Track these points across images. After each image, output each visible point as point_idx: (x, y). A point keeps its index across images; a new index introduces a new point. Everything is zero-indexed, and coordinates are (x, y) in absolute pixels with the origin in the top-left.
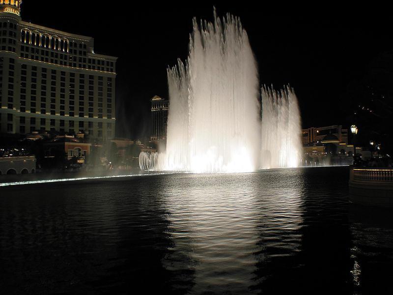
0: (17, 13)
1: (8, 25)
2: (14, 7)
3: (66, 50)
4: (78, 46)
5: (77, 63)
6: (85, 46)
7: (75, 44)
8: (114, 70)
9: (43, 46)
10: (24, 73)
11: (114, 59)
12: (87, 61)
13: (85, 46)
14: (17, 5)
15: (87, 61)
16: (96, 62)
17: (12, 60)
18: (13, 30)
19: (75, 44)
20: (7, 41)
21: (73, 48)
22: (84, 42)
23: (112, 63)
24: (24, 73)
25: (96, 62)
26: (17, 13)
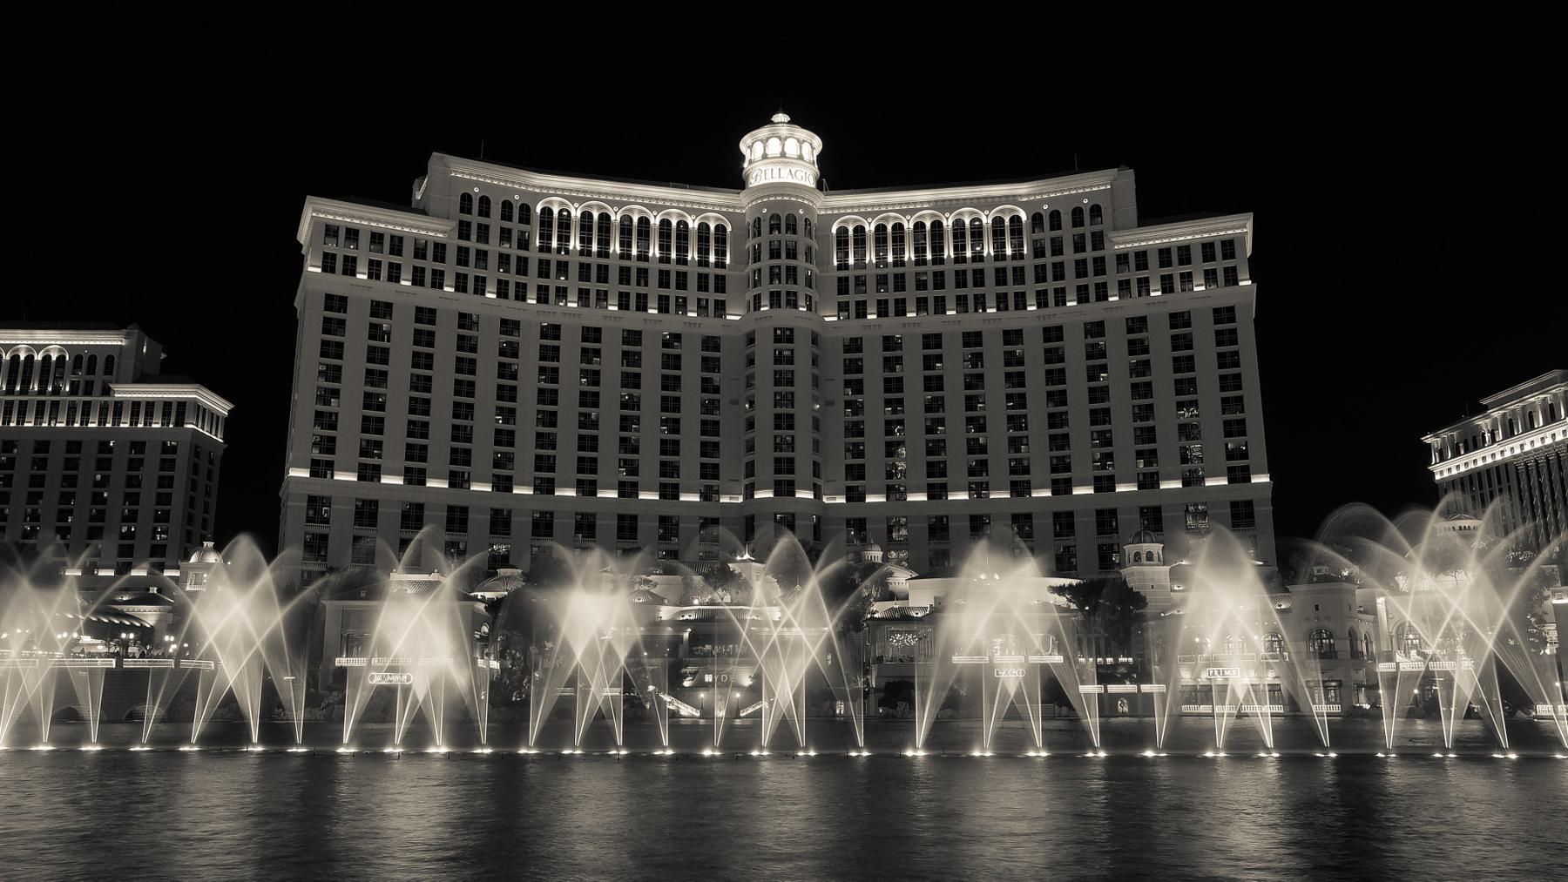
0: (806, 175)
1: (765, 227)
3: (1018, 246)
4: (1066, 220)
7: (1055, 216)
10: (853, 366)
11: (1240, 227)
13: (1096, 211)
15: (1111, 265)
16: (1153, 261)
17: (785, 336)
18: (784, 237)
21: (1047, 235)
23: (1229, 247)
24: (853, 366)
25: (1153, 261)
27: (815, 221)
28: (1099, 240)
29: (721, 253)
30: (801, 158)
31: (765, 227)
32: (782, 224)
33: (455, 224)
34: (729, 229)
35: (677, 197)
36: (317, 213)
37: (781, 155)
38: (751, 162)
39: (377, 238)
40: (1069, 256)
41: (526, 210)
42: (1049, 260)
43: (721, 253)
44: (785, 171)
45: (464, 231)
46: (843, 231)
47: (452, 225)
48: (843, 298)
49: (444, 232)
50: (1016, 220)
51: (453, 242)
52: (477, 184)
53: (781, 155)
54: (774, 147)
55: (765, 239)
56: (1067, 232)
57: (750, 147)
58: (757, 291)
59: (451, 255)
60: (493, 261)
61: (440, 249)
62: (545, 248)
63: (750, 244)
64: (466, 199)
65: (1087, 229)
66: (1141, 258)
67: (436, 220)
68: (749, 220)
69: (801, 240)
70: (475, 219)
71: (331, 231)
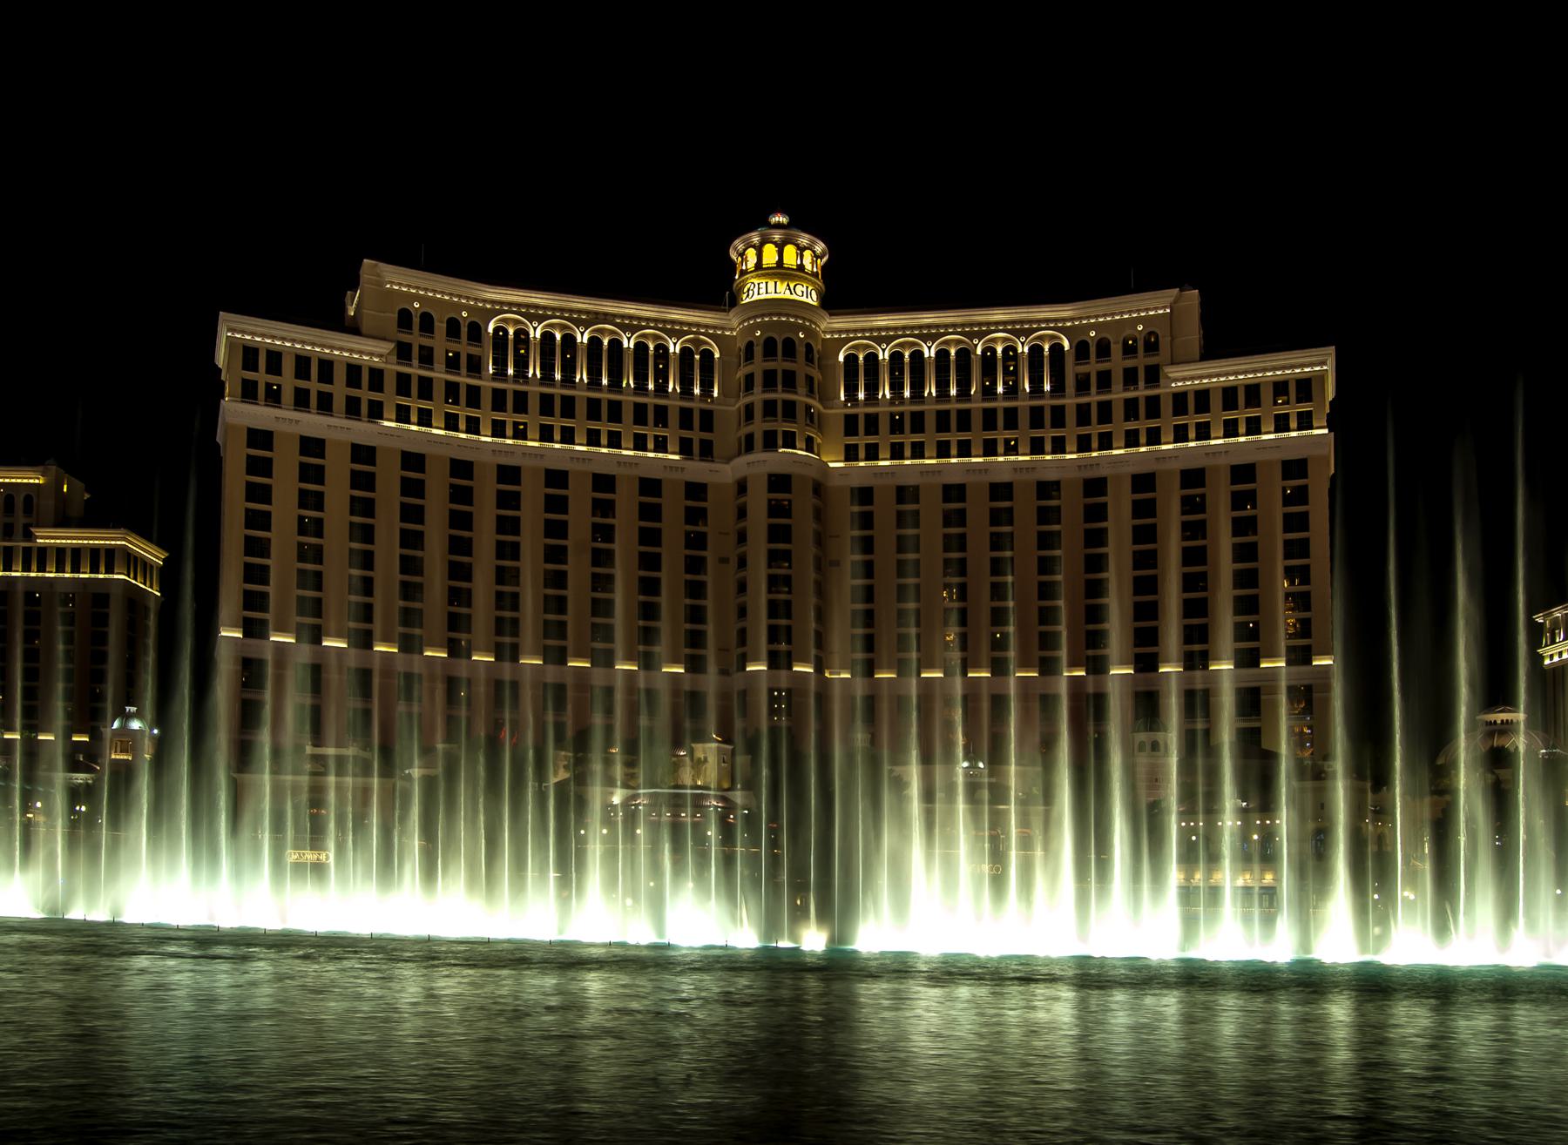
0: (807, 294)
1: (758, 351)
2: (780, 271)
4: (1117, 350)
5: (1119, 426)
6: (1152, 346)
7: (1104, 349)
8: (1320, 419)
9: (594, 381)
12: (1167, 407)
14: (808, 267)
15: (1167, 407)
16: (1216, 401)
17: (779, 482)
18: (779, 365)
19: (1104, 349)
20: (758, 412)
22: (1145, 321)
23: (1305, 388)
25: (1216, 401)
26: (807, 294)
27: (817, 347)
28: (1153, 376)
29: (707, 386)
30: (801, 268)
31: (758, 351)
32: (782, 350)
33: (392, 346)
34: (717, 355)
35: (653, 315)
36: (234, 331)
37: (778, 270)
38: (743, 273)
39: (303, 362)
40: (1118, 395)
41: (476, 332)
42: (1094, 398)
43: (707, 386)
44: (782, 287)
45: (403, 352)
46: (851, 359)
47: (387, 347)
48: (852, 441)
49: (380, 356)
50: (1057, 349)
51: (393, 367)
52: (417, 298)
53: (778, 270)
54: (770, 255)
55: (758, 366)
56: (1117, 363)
57: (742, 255)
58: (749, 429)
59: (390, 384)
60: (439, 391)
61: (377, 376)
62: (500, 373)
63: (741, 374)
64: (405, 318)
65: (1141, 361)
66: (1203, 397)
67: (371, 342)
68: (741, 344)
69: (800, 367)
70: (416, 339)
71: (249, 356)
